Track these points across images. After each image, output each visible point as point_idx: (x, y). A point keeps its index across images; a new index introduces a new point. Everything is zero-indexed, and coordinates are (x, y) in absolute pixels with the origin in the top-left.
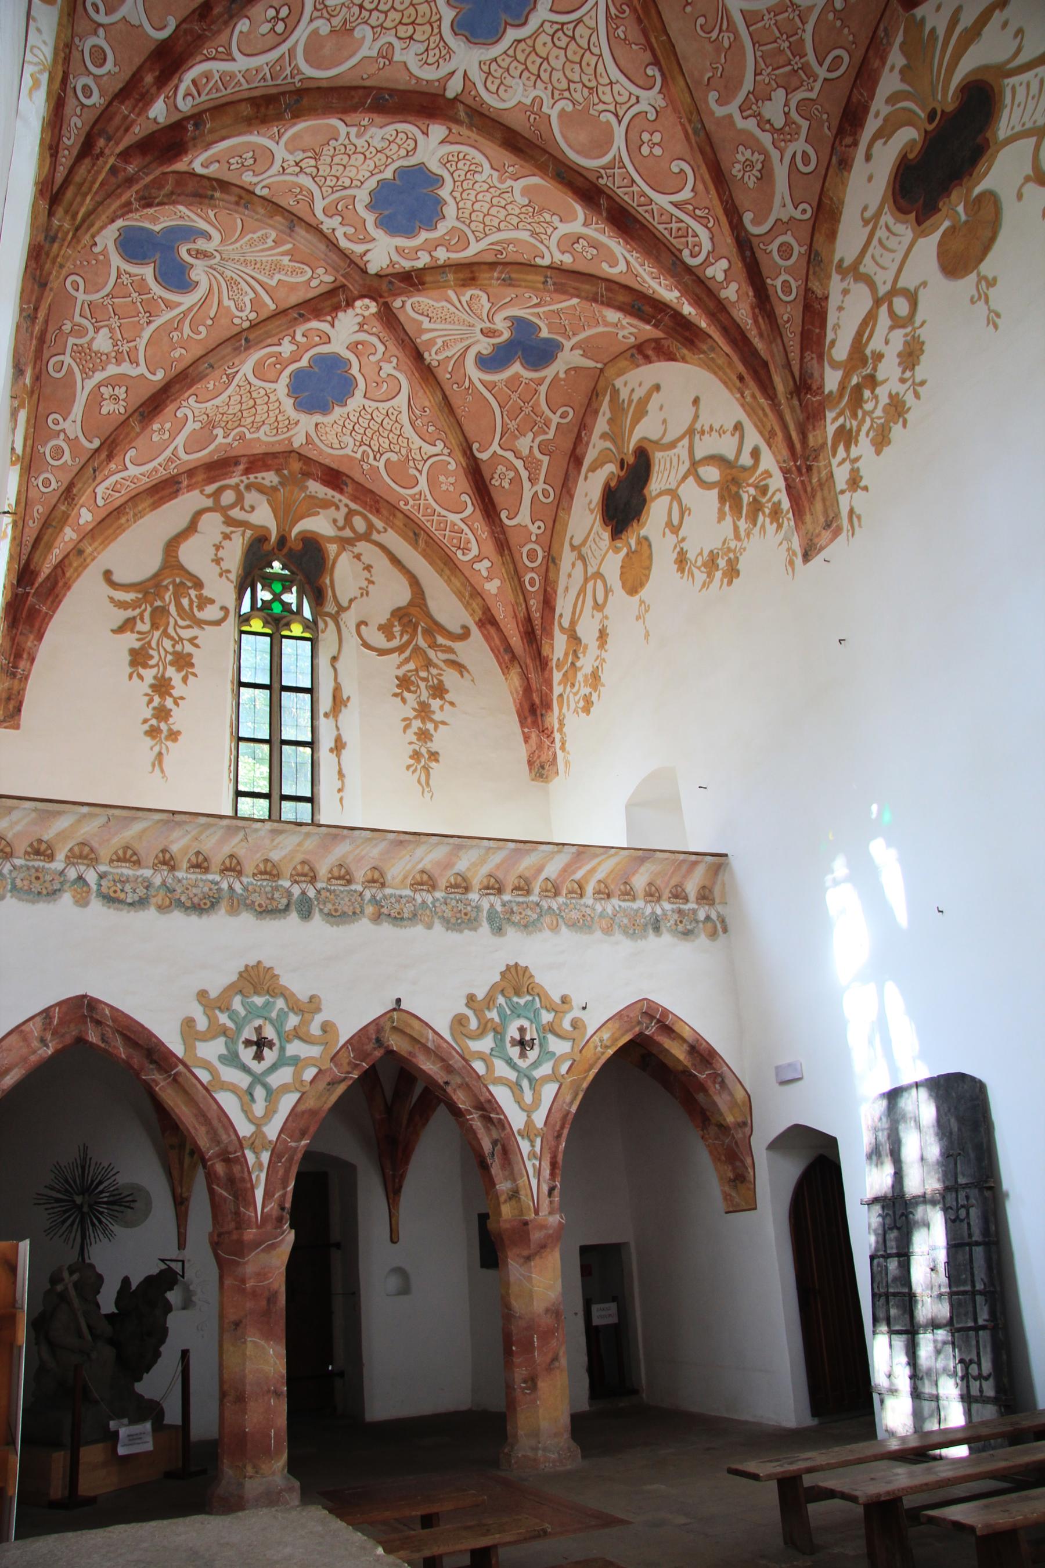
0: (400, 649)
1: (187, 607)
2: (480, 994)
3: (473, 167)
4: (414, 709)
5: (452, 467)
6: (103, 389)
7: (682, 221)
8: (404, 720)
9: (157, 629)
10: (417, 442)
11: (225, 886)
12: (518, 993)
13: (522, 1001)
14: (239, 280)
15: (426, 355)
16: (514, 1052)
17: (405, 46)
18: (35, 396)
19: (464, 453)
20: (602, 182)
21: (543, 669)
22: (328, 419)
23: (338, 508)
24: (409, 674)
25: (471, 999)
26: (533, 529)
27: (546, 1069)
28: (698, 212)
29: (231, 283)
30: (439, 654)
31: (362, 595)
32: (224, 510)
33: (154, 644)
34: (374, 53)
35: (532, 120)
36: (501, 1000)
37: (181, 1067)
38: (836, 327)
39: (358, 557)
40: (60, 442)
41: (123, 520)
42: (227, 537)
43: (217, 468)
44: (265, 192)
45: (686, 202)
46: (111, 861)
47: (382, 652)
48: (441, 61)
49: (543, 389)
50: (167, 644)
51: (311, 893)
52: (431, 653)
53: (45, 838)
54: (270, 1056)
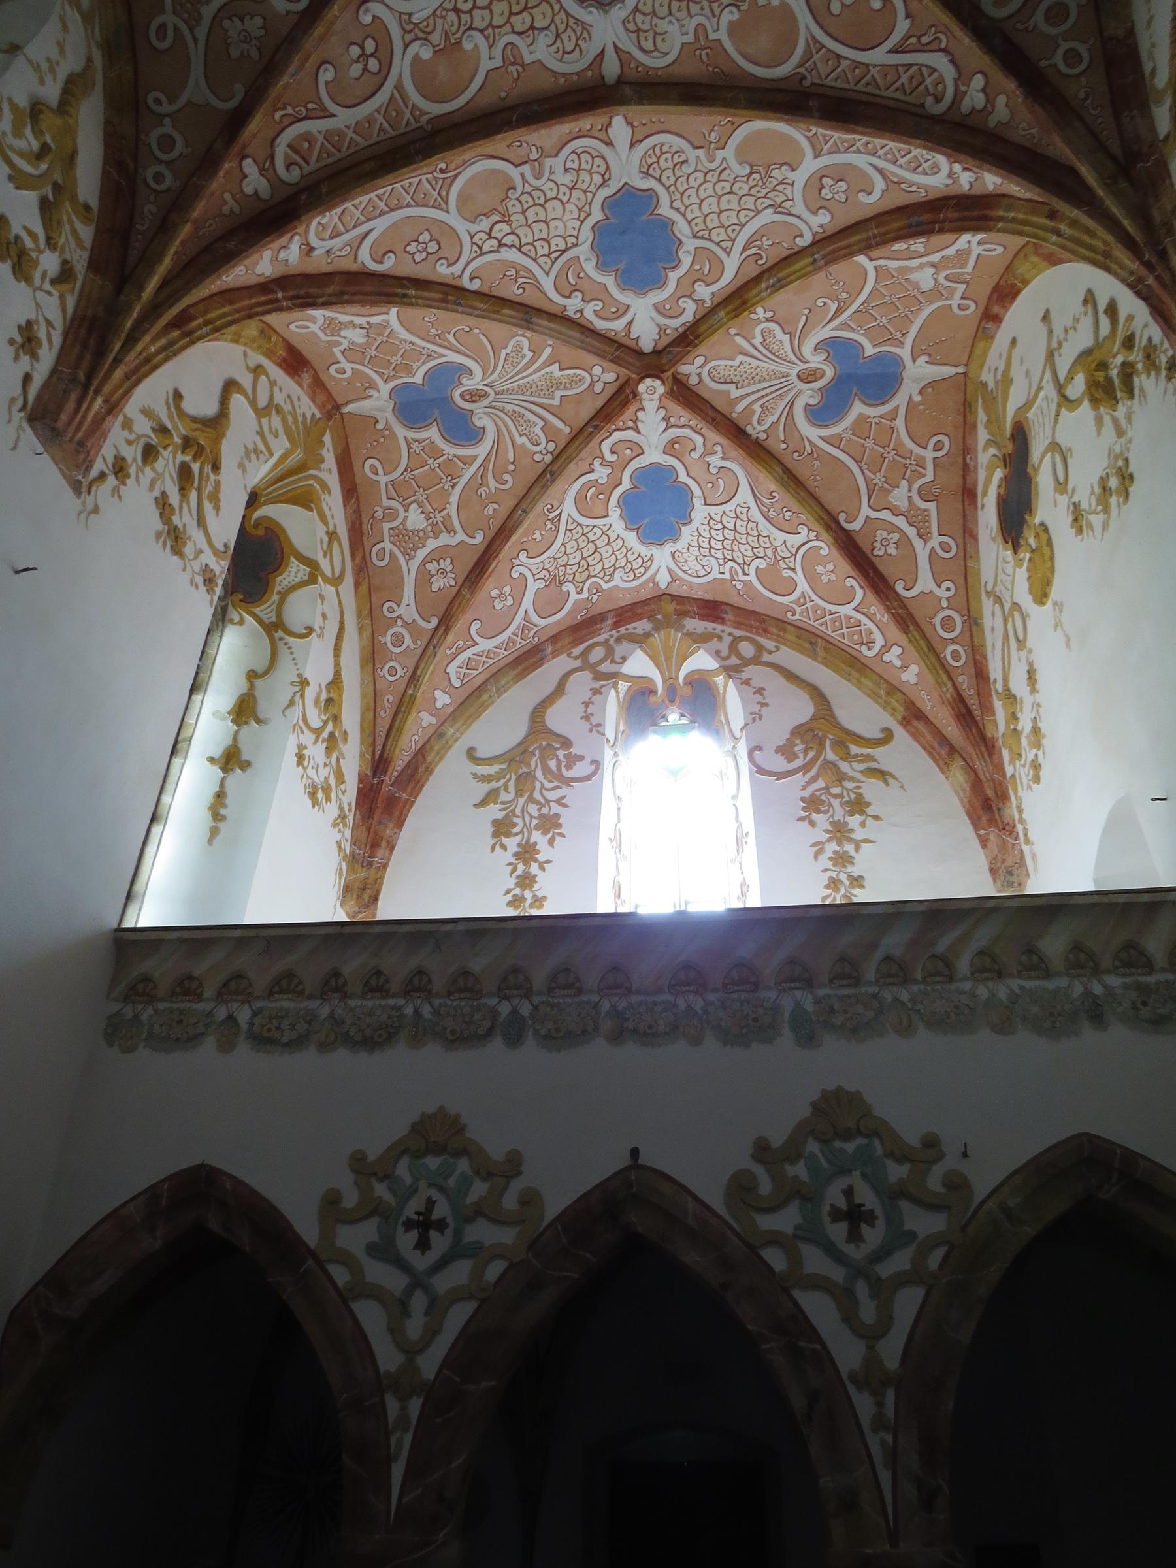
0: (805, 768)
1: (554, 768)
2: (777, 1140)
3: (676, 159)
4: (826, 831)
5: (825, 551)
6: (429, 566)
7: (911, 65)
8: (814, 845)
9: (522, 796)
10: (779, 536)
11: (409, 1010)
12: (846, 1136)
13: (850, 1147)
14: (523, 411)
15: (749, 429)
16: (838, 1231)
17: (530, 40)
18: (364, 588)
19: (828, 528)
20: (806, 83)
21: (991, 755)
22: (681, 545)
23: (720, 638)
24: (818, 793)
25: (762, 1150)
26: (941, 593)
27: (901, 1261)
28: (925, 40)
29: (515, 417)
30: (855, 765)
31: (754, 720)
32: (592, 667)
33: (518, 812)
34: (498, 62)
35: (705, 58)
36: (812, 1146)
37: (310, 1262)
38: (1151, 57)
39: (747, 682)
40: (399, 628)
41: (485, 697)
42: (596, 692)
43: (583, 628)
44: (475, 285)
45: (907, 37)
46: (271, 994)
47: (782, 775)
48: (580, 42)
49: (900, 423)
50: (533, 809)
51: (525, 1010)
52: (844, 766)
53: (197, 972)
54: (440, 1243)
